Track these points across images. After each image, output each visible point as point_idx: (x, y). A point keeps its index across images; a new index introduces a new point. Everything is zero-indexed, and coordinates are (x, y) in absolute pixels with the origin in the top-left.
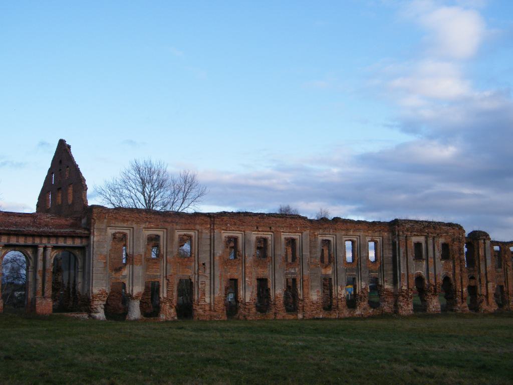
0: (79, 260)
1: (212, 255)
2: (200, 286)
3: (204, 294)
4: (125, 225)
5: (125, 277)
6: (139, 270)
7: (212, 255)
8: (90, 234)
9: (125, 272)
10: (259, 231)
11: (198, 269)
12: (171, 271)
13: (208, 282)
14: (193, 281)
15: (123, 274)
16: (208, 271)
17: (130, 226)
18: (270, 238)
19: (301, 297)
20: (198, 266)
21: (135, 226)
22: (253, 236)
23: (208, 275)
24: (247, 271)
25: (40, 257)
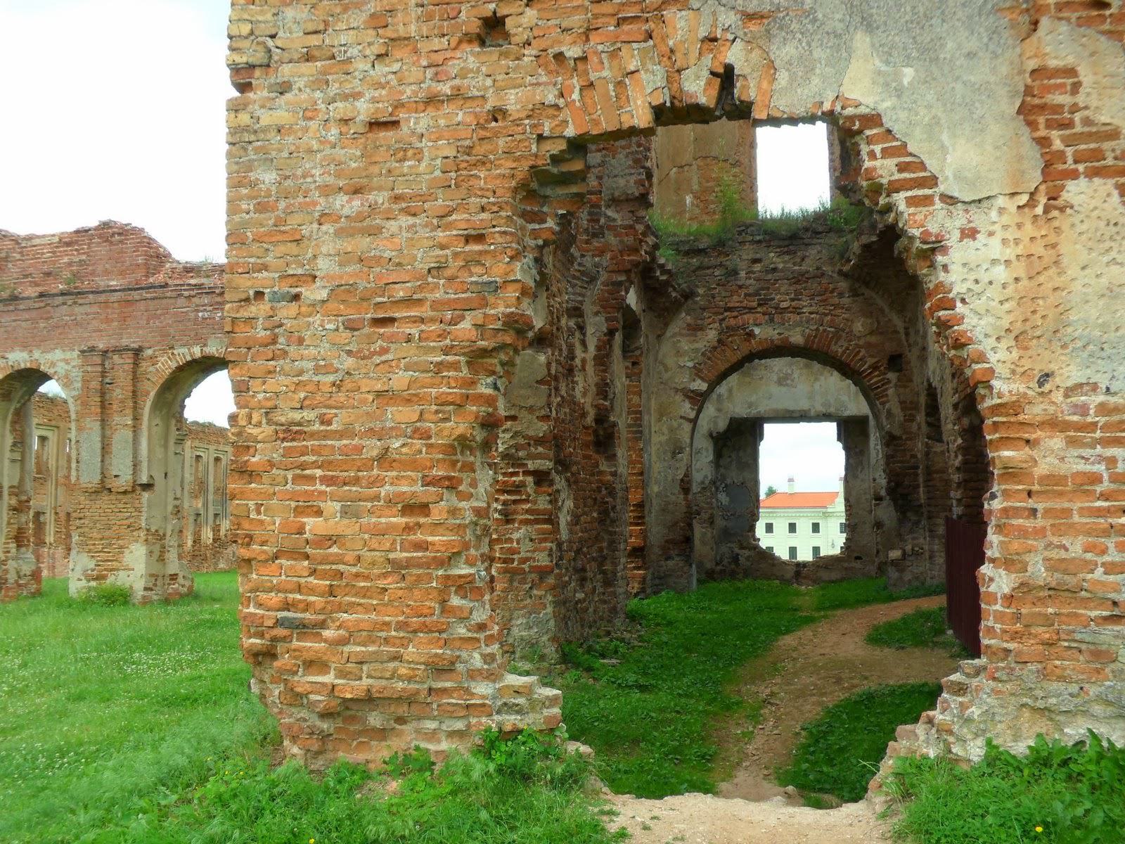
12: (61, 500)
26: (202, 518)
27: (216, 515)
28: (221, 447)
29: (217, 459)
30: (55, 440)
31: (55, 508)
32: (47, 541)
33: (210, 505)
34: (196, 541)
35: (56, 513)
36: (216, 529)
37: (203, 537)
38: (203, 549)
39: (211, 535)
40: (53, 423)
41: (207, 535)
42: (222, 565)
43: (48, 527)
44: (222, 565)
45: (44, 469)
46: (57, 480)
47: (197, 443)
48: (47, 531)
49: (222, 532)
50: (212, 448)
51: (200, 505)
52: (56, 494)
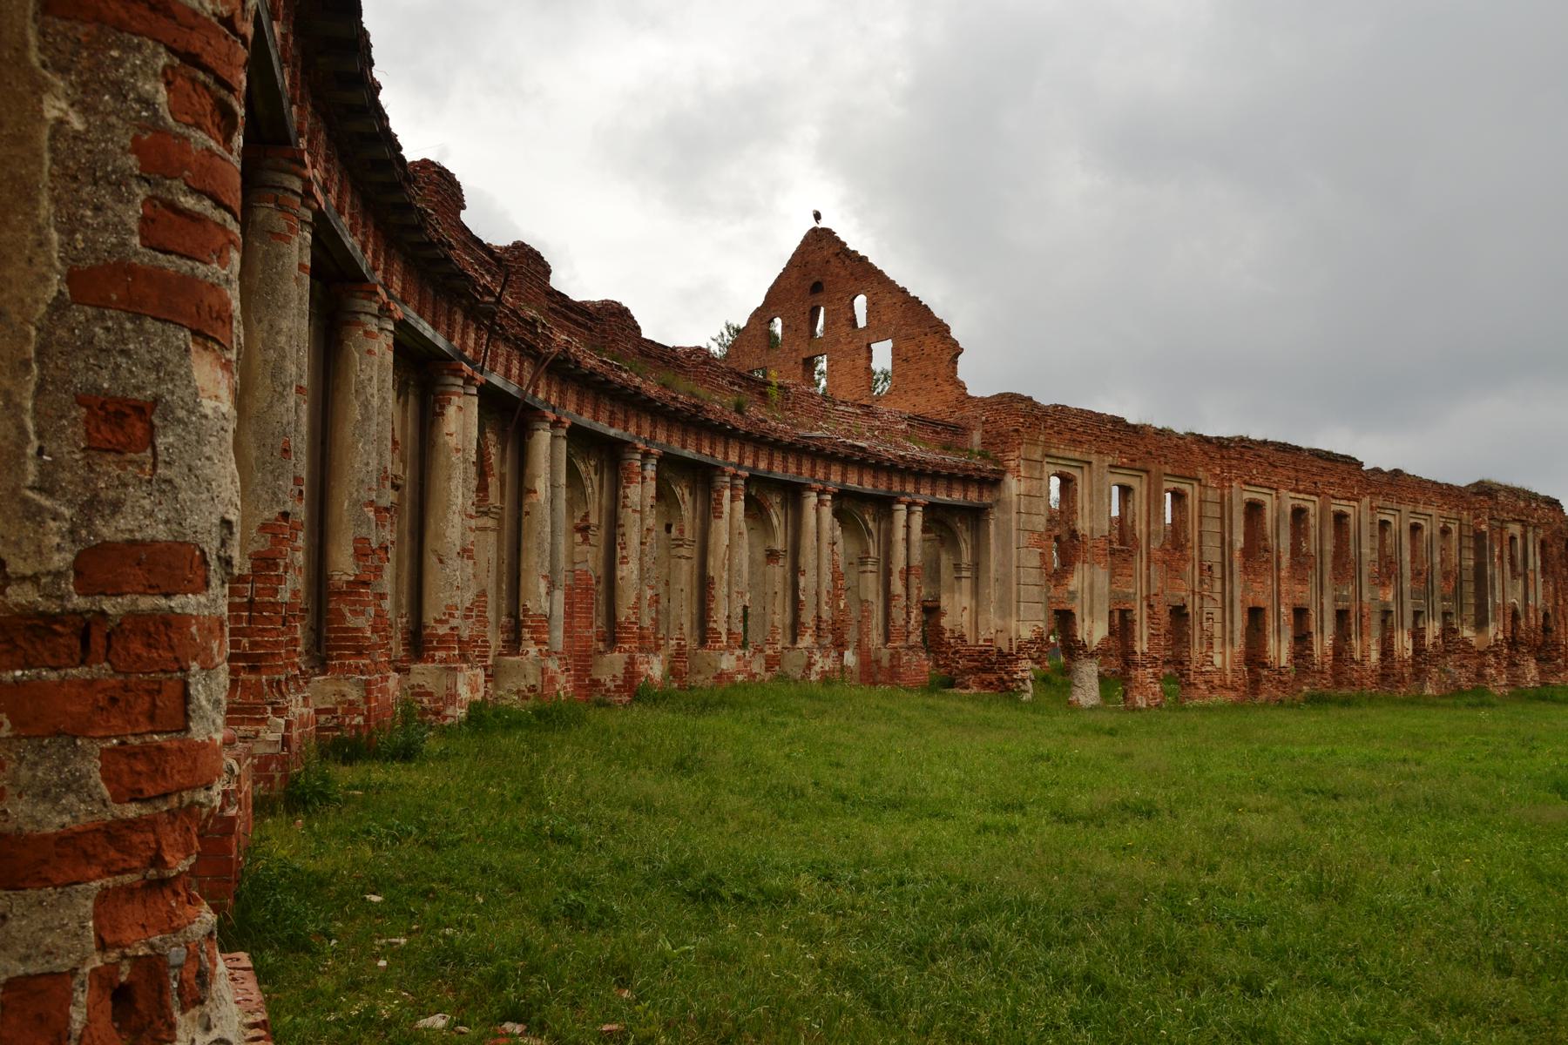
0: (963, 545)
1: (1225, 544)
2: (1205, 625)
3: (1211, 646)
4: (1077, 455)
5: (1073, 595)
6: (1101, 576)
7: (1225, 544)
8: (1003, 473)
9: (1075, 582)
10: (1299, 492)
11: (1201, 582)
12: (1157, 585)
13: (1217, 615)
14: (1189, 610)
15: (1071, 588)
16: (1218, 585)
17: (1086, 458)
18: (1311, 511)
19: (1357, 656)
20: (1201, 574)
21: (1094, 458)
22: (1289, 500)
23: (1218, 597)
24: (1284, 587)
25: (900, 533)
26: (1394, 619)
27: (1417, 614)
28: (1420, 509)
29: (1415, 528)
30: (1145, 493)
31: (1148, 597)
32: (1137, 649)
33: (1407, 598)
34: (1386, 651)
35: (1150, 606)
36: (1418, 635)
37: (1397, 646)
38: (1397, 665)
39: (1409, 644)
40: (1138, 464)
41: (1403, 643)
42: (1429, 690)
43: (1137, 628)
44: (1429, 690)
45: (1128, 538)
46: (1148, 553)
47: (1379, 502)
48: (1137, 634)
49: (1429, 639)
50: (1406, 508)
51: (1390, 597)
52: (1149, 576)
